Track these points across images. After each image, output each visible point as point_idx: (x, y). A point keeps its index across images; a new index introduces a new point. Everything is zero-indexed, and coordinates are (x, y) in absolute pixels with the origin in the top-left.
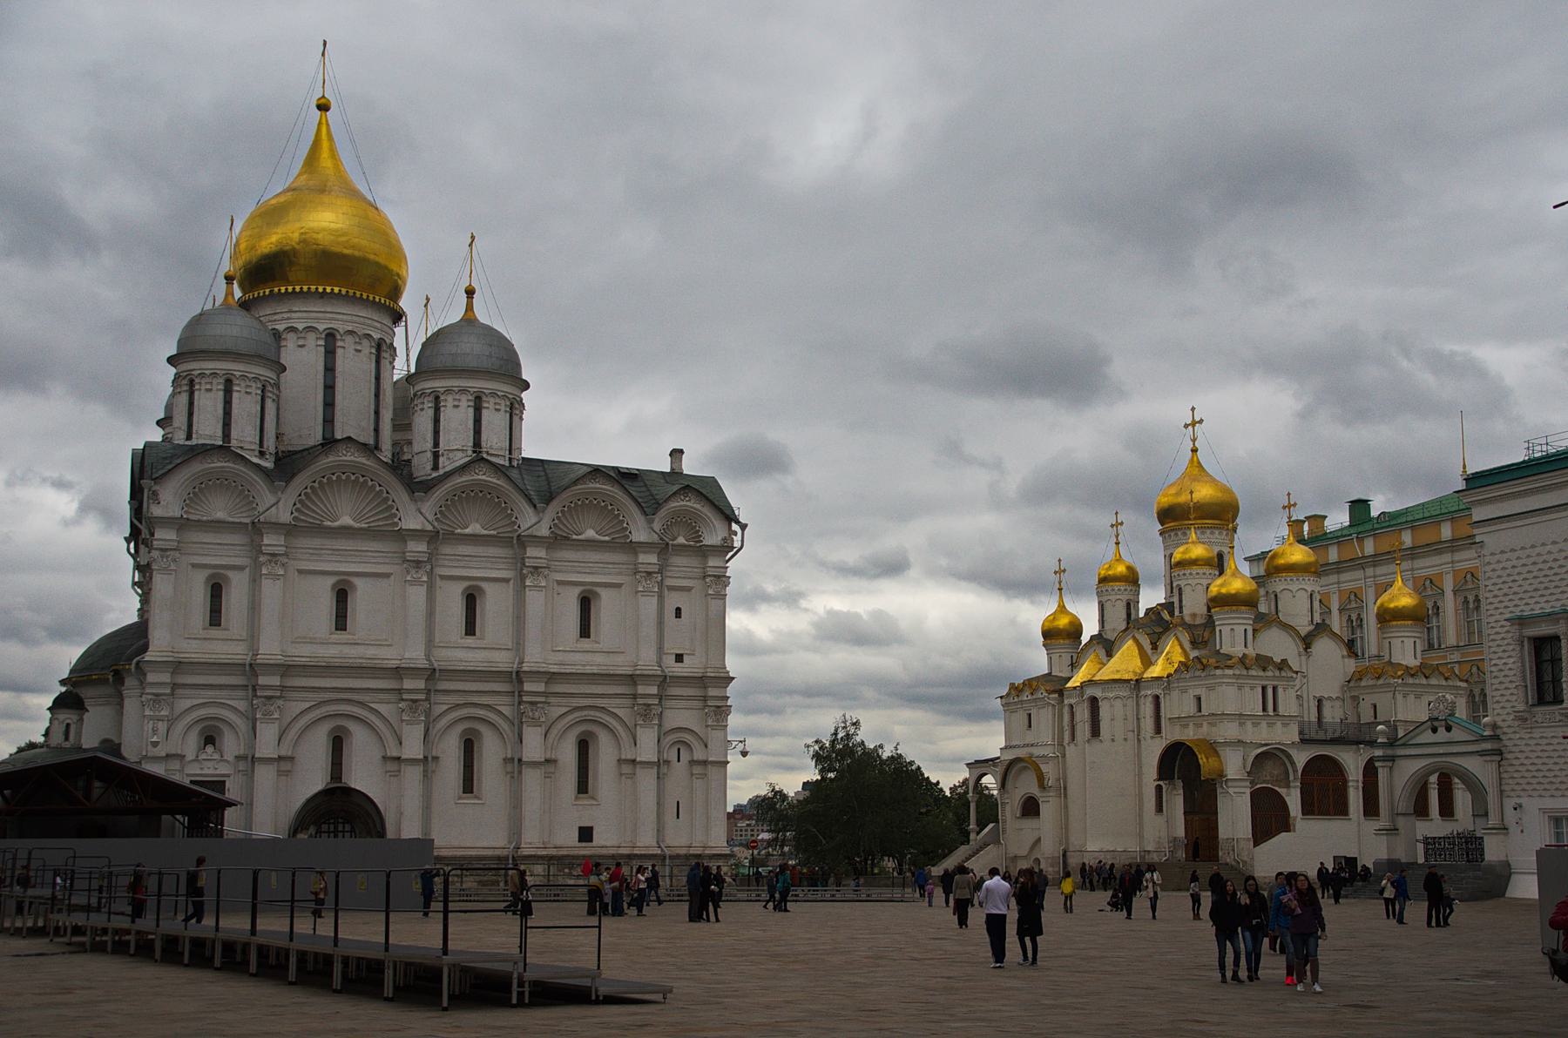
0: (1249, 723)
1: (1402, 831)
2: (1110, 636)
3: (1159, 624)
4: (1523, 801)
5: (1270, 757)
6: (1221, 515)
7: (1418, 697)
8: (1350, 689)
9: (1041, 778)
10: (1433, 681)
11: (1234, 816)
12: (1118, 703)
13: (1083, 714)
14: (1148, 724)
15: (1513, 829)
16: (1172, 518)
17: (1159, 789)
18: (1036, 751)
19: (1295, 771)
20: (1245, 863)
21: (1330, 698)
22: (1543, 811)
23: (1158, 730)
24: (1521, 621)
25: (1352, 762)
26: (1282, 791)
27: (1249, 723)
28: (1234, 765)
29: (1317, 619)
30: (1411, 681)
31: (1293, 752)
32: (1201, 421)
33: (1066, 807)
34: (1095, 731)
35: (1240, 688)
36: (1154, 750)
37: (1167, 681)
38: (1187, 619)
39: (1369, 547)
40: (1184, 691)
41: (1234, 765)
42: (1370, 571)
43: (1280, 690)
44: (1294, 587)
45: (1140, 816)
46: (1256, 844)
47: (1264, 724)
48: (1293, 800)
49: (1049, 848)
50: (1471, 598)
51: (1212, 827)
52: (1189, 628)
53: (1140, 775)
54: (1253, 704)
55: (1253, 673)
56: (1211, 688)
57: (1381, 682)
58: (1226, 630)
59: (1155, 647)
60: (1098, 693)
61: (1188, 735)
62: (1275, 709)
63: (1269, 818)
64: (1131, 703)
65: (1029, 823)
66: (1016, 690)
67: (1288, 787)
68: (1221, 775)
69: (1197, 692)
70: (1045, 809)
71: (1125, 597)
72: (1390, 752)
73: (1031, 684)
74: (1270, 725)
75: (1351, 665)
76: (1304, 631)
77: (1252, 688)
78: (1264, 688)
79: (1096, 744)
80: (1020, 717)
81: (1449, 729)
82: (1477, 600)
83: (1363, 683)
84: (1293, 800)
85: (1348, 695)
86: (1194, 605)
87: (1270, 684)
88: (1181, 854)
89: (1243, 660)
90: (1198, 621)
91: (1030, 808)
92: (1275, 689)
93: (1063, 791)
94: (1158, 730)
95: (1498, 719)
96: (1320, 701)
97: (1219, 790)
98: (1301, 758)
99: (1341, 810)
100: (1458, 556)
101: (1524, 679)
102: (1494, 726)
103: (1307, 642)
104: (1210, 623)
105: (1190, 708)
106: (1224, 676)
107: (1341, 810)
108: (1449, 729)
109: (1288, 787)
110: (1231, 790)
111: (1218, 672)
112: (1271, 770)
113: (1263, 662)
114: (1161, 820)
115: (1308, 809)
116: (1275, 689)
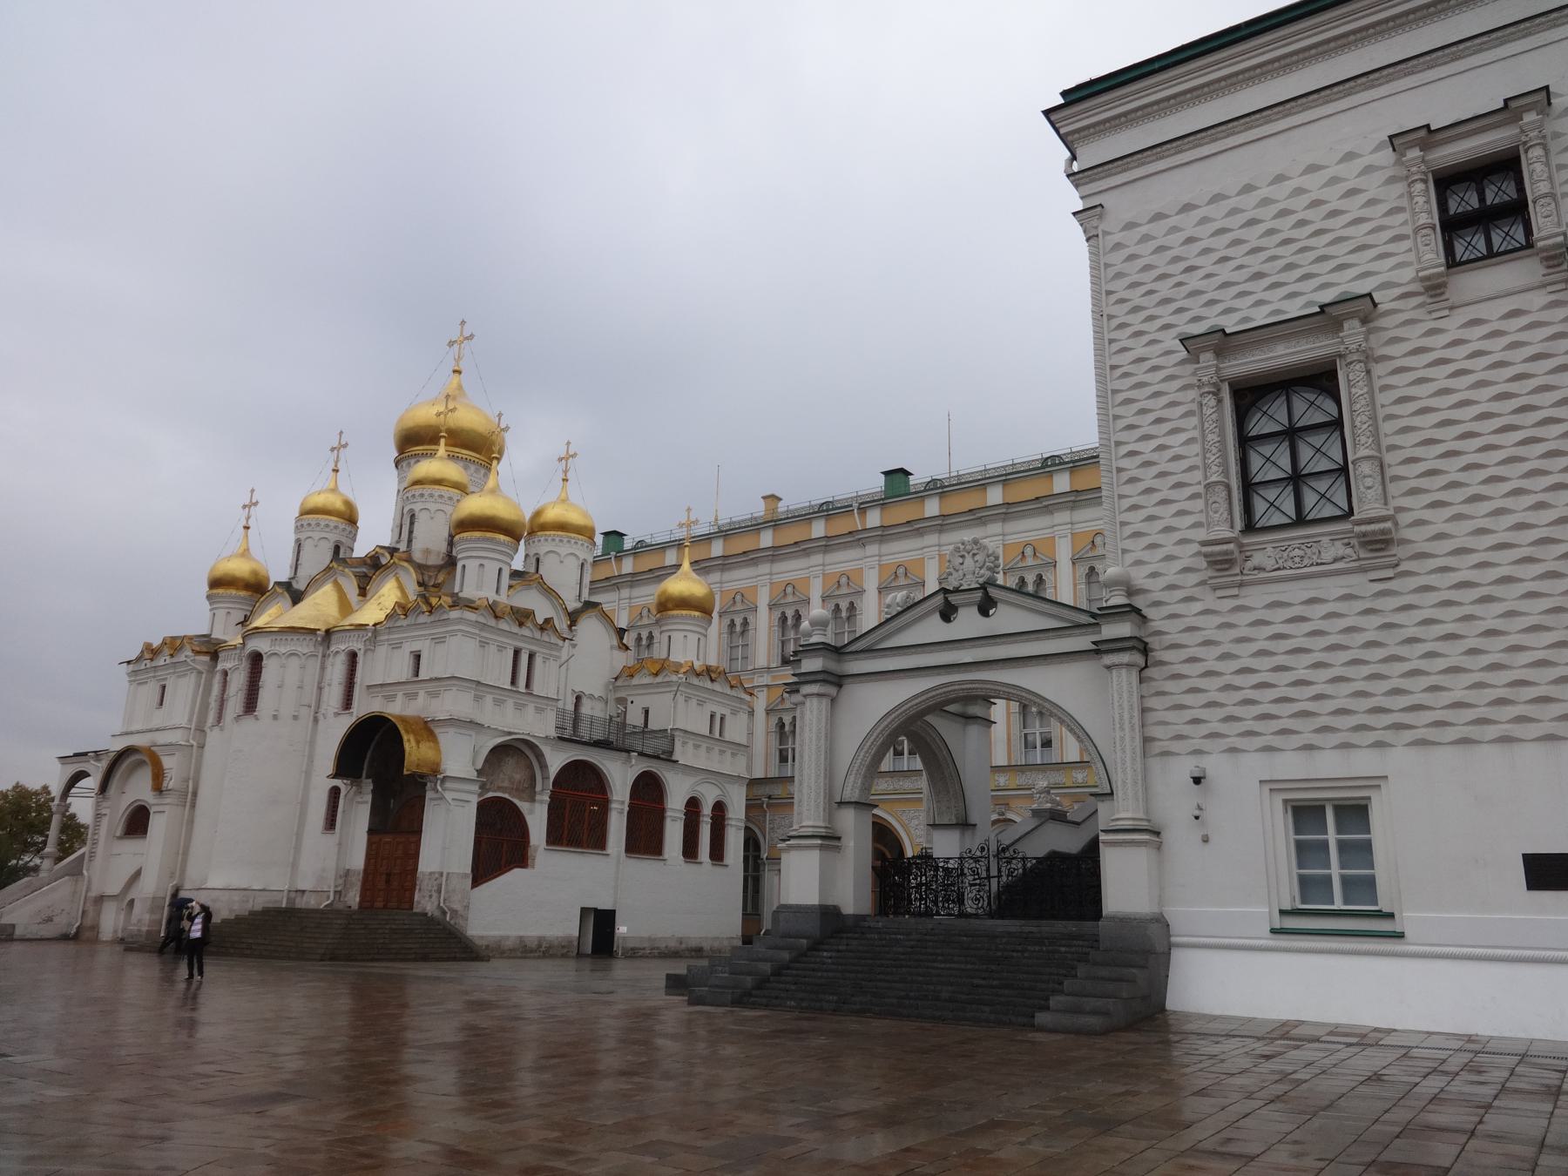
0: (489, 699)
1: (849, 843)
2: (300, 585)
3: (372, 569)
4: (1214, 764)
5: (512, 752)
6: (479, 448)
7: (701, 703)
8: (616, 689)
9: (158, 776)
10: (717, 687)
11: (447, 838)
12: (294, 663)
13: (238, 681)
14: (334, 694)
15: (1180, 834)
16: (413, 441)
17: (335, 792)
18: (162, 738)
19: (545, 778)
20: (454, 912)
21: (591, 697)
22: (1273, 785)
23: (347, 703)
24: (1222, 342)
25: (620, 775)
26: (523, 806)
27: (489, 699)
28: (459, 758)
29: (585, 596)
30: (695, 681)
31: (546, 750)
32: (471, 337)
33: (191, 821)
34: (251, 704)
35: (483, 644)
36: (336, 729)
37: (374, 633)
38: (417, 556)
39: (628, 566)
40: (397, 646)
41: (459, 758)
42: (625, 593)
43: (538, 660)
44: (564, 550)
45: (299, 836)
46: (477, 882)
47: (510, 703)
48: (537, 819)
49: (152, 886)
50: (738, 621)
51: (412, 855)
52: (420, 568)
53: (308, 774)
54: (498, 671)
55: (503, 625)
56: (439, 640)
57: (659, 679)
58: (472, 566)
59: (363, 592)
60: (261, 645)
61: (395, 708)
62: (528, 686)
63: (499, 845)
64: (314, 665)
65: (132, 845)
66: (151, 652)
67: (532, 800)
68: (435, 770)
69: (416, 646)
70: (157, 824)
71: (333, 537)
72: (832, 666)
73: (174, 645)
74: (519, 707)
75: (622, 660)
76: (573, 605)
77: (501, 648)
78: (517, 653)
79: (248, 722)
80: (151, 690)
81: (984, 611)
82: (745, 623)
83: (635, 681)
84: (537, 819)
85: (612, 697)
86: (431, 538)
87: (526, 648)
88: (353, 898)
89: (494, 610)
90: (435, 560)
91: (137, 822)
92: (531, 656)
93: (190, 797)
94: (347, 703)
95: (1139, 577)
96: (578, 698)
97: (429, 794)
98: (556, 760)
99: (595, 840)
100: (728, 576)
101: (1226, 473)
102: (1131, 591)
103: (573, 618)
104: (450, 562)
105: (400, 668)
106: (460, 620)
107: (595, 840)
108: (986, 607)
109: (532, 800)
110: (449, 796)
111: (455, 614)
112: (512, 771)
113: (522, 617)
114: (332, 839)
115: (559, 836)
116: (531, 656)
